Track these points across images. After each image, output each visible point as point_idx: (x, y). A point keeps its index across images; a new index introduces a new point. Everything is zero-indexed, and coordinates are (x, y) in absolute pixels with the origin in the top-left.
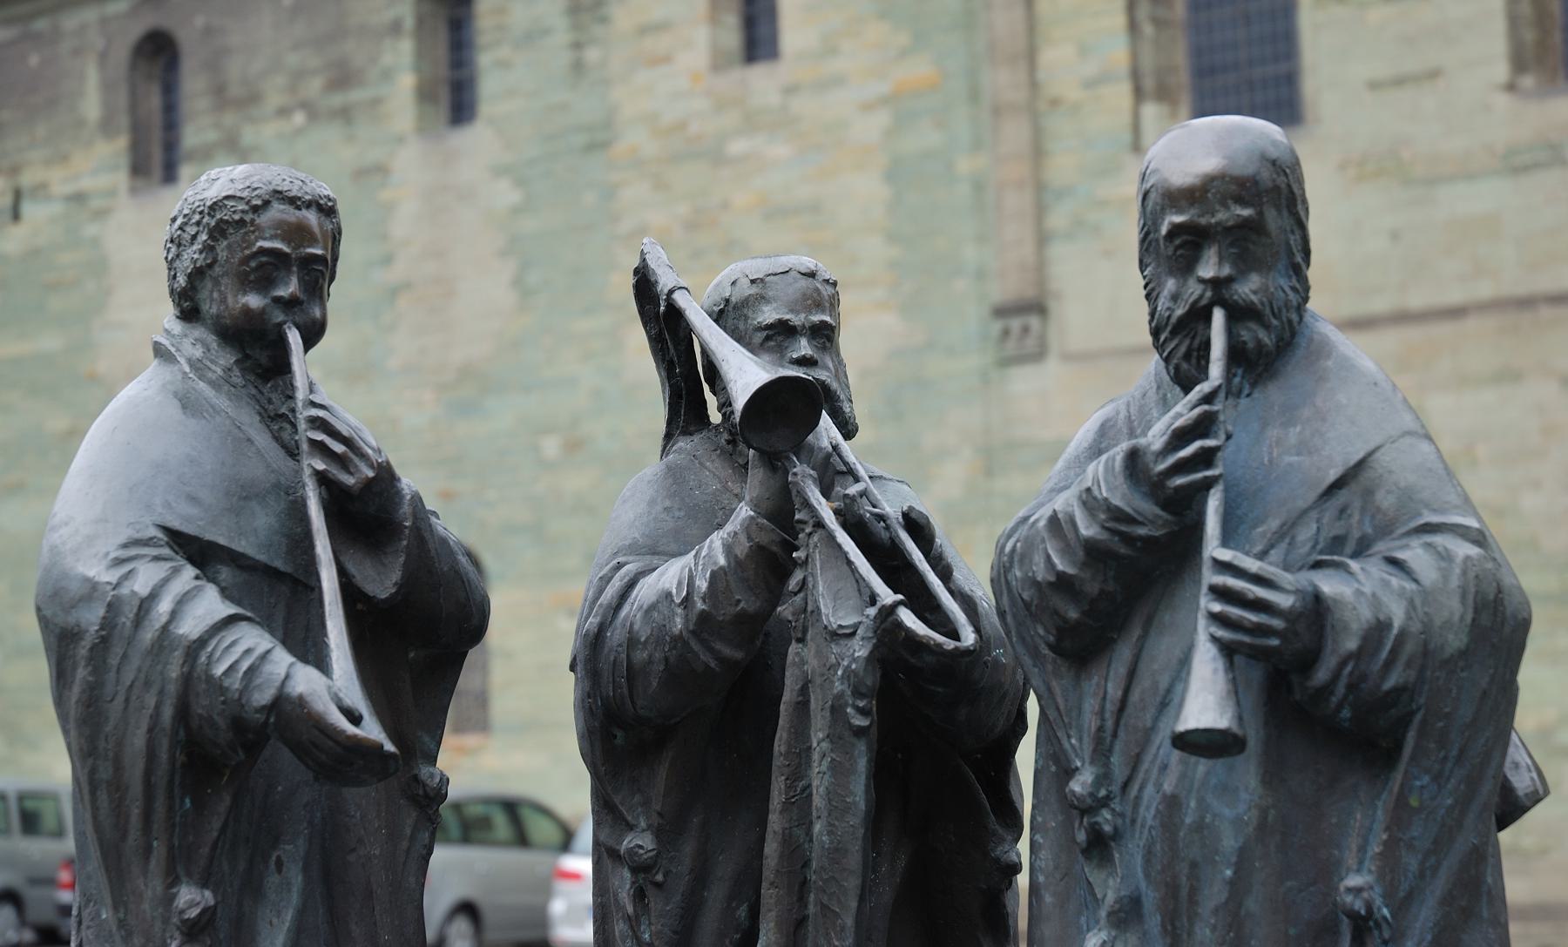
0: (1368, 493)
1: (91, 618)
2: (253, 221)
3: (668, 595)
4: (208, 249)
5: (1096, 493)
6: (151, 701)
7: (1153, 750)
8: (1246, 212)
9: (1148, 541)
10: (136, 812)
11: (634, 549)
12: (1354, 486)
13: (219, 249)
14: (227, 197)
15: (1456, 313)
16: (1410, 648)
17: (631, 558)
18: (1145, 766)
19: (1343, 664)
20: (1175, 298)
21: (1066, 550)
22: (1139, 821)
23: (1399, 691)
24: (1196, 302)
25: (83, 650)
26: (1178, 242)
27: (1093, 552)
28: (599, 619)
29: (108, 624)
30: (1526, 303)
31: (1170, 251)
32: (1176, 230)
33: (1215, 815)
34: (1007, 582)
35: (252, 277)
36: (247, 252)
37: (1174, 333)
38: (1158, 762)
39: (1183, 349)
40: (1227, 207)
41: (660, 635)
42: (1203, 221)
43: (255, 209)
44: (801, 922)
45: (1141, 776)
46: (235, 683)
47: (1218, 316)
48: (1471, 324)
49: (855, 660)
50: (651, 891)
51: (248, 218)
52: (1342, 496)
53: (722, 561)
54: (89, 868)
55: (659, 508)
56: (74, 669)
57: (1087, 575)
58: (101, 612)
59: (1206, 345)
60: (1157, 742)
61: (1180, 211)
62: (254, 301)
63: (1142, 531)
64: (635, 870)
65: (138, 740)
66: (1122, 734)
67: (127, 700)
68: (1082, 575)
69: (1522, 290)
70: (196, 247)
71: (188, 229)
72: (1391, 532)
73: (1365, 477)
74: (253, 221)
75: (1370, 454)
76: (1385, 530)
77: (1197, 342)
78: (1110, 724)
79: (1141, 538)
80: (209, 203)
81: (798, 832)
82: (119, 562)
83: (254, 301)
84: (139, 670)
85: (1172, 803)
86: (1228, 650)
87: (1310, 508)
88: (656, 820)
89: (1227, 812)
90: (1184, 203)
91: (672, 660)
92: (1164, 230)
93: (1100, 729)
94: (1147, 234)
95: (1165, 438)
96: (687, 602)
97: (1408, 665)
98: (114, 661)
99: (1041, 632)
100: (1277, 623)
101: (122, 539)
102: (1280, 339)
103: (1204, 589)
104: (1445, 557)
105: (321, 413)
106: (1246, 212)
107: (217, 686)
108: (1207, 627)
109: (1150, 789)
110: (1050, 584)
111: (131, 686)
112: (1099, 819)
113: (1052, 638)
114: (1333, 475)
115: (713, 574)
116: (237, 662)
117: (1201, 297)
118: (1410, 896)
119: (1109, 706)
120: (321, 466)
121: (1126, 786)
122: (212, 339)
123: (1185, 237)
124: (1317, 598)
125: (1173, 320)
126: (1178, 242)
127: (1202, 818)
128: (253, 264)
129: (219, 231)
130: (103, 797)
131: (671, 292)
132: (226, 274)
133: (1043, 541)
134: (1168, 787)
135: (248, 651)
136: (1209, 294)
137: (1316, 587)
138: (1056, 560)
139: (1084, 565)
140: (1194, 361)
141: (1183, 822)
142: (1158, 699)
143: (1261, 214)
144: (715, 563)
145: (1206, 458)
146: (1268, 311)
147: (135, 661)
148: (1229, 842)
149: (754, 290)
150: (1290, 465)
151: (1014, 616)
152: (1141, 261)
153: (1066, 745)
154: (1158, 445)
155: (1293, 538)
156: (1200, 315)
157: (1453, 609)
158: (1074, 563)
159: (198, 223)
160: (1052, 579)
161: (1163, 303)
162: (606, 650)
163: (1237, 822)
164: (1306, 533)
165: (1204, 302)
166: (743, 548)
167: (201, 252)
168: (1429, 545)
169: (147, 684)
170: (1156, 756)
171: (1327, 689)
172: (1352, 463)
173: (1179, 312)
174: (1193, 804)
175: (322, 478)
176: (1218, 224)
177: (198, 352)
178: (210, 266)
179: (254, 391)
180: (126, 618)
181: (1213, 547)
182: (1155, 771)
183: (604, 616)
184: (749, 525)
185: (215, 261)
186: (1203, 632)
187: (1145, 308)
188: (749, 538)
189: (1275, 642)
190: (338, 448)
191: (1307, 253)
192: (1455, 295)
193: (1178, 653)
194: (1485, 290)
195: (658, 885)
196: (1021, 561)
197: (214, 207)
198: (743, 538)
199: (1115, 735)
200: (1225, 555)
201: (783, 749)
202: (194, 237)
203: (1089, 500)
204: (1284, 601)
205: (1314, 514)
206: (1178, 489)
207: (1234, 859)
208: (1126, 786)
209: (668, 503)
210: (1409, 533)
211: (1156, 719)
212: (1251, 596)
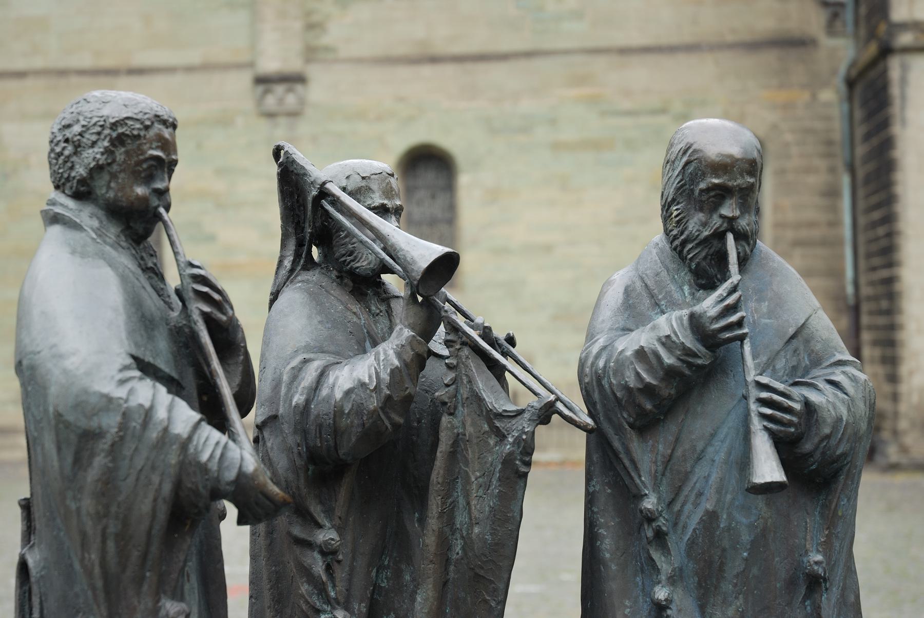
0: (807, 341)
1: (111, 422)
2: (145, 136)
3: (363, 385)
4: (107, 151)
5: (674, 338)
6: (156, 479)
7: (691, 484)
8: (752, 180)
9: (701, 367)
10: (135, 554)
11: (307, 348)
12: (800, 338)
13: (117, 154)
14: (128, 118)
15: (20, 75)
16: (849, 431)
17: (312, 356)
18: (685, 492)
19: (822, 441)
20: (704, 224)
21: (650, 370)
22: (681, 525)
23: (844, 455)
24: (717, 228)
25: (104, 445)
26: (712, 194)
27: (670, 373)
28: (303, 398)
29: (123, 426)
30: (63, 73)
33: (737, 523)
35: (143, 175)
36: (141, 157)
38: (695, 492)
39: (703, 254)
40: (743, 177)
41: (358, 410)
42: (730, 184)
43: (147, 128)
44: (445, 584)
45: (681, 499)
46: (213, 466)
47: (730, 237)
48: (29, 82)
49: (526, 433)
50: (336, 567)
51: (142, 133)
52: (795, 342)
53: (396, 362)
54: (77, 589)
55: (315, 322)
56: (92, 455)
57: (663, 385)
58: (118, 419)
60: (695, 479)
61: (717, 177)
62: (140, 190)
63: (700, 362)
64: (323, 553)
65: (145, 507)
66: (668, 474)
67: (137, 479)
68: (661, 385)
69: (62, 64)
70: (98, 149)
71: (87, 136)
72: (821, 364)
73: (806, 331)
74: (145, 136)
75: (807, 320)
76: (816, 362)
78: (660, 468)
80: (113, 121)
81: (447, 529)
82: (122, 382)
83: (140, 190)
84: (148, 459)
85: (712, 517)
86: (772, 434)
87: (781, 350)
88: (337, 522)
89: (744, 520)
91: (367, 426)
93: (656, 472)
94: (682, 186)
96: (377, 389)
97: (848, 441)
98: (127, 452)
99: (625, 416)
100: (795, 419)
101: (118, 366)
104: (853, 379)
105: (196, 271)
107: (203, 468)
108: (760, 422)
109: (689, 507)
110: (639, 389)
111: (141, 470)
112: (659, 523)
114: (791, 331)
115: (392, 371)
116: (213, 451)
117: (721, 226)
118: (834, 564)
119: (659, 458)
120: (207, 309)
121: (670, 504)
122: (101, 213)
124: (807, 404)
126: (712, 194)
127: (730, 524)
128: (145, 166)
129: (119, 141)
130: (111, 545)
131: (324, 183)
132: (123, 171)
133: (632, 363)
134: (709, 506)
135: (217, 443)
137: (806, 398)
138: (644, 375)
139: (662, 380)
140: (708, 261)
141: (719, 526)
142: (696, 456)
144: (392, 364)
145: (739, 324)
147: (144, 453)
148: (746, 537)
149: (364, 184)
150: (766, 324)
151: (604, 406)
153: (638, 481)
155: (774, 366)
156: (720, 236)
157: (861, 408)
158: (655, 378)
159: (99, 133)
160: (640, 386)
161: (693, 225)
162: (312, 417)
163: (751, 526)
164: (780, 364)
165: (722, 229)
166: (409, 355)
167: (102, 154)
168: (844, 373)
169: (153, 468)
170: (693, 488)
171: (810, 454)
174: (725, 516)
175: (207, 318)
176: (737, 186)
177: (96, 223)
178: (109, 164)
179: (134, 252)
180: (136, 424)
181: (752, 375)
182: (692, 498)
183: (308, 394)
184: (411, 341)
185: (114, 161)
186: (757, 424)
187: (661, 225)
188: (413, 349)
189: (793, 430)
190: (217, 297)
192: (20, 64)
193: (709, 430)
194: (38, 63)
195: (339, 562)
197: (114, 126)
198: (408, 348)
199: (663, 474)
200: (764, 380)
201: (440, 480)
202: (94, 144)
203: (667, 342)
204: (797, 406)
205: (782, 353)
207: (748, 547)
208: (670, 504)
209: (319, 318)
210: (831, 365)
211: (693, 467)
212: (786, 405)
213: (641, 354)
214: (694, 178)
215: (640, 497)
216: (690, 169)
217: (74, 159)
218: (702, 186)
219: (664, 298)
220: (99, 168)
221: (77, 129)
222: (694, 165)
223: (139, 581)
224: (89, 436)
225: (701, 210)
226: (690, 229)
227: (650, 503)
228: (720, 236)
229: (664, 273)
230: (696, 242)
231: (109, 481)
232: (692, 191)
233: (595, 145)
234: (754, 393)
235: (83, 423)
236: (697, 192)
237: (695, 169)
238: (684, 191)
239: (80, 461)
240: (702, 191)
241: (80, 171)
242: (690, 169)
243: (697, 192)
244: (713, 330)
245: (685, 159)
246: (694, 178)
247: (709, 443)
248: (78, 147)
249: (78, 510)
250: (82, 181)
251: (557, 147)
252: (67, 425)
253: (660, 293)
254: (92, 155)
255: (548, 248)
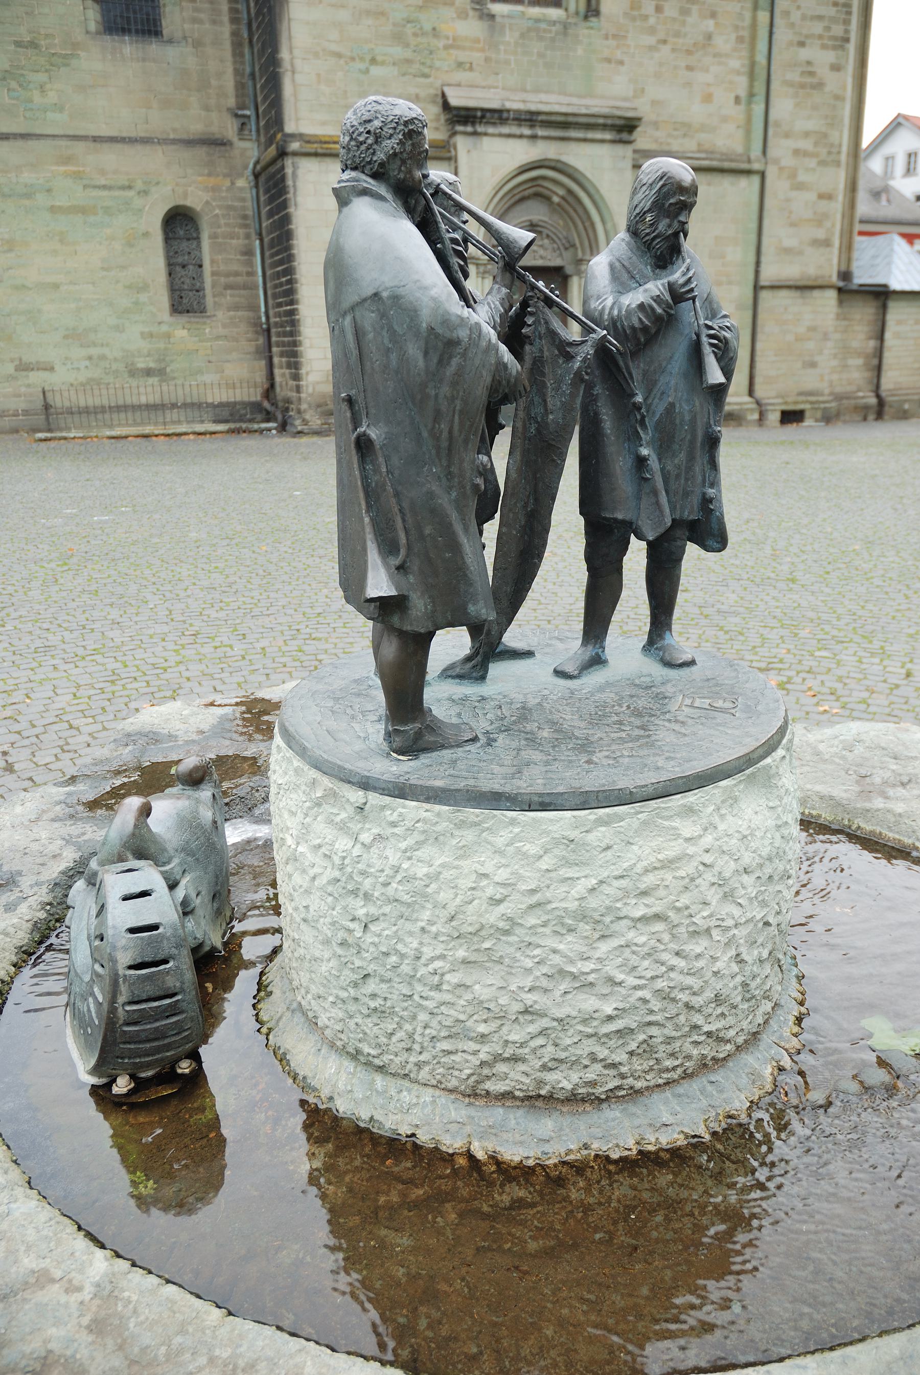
4: (401, 143)
20: (669, 226)
21: (647, 317)
25: (460, 350)
45: (652, 396)
54: (424, 449)
56: (451, 357)
70: (394, 141)
85: (672, 405)
132: (410, 158)
159: (395, 128)
197: (406, 123)
203: (657, 299)
213: (641, 306)
214: (667, 196)
215: (634, 395)
216: (665, 189)
217: (375, 147)
218: (672, 201)
220: (395, 154)
221: (377, 123)
223: (466, 441)
224: (452, 343)
225: (668, 217)
227: (639, 399)
229: (634, 258)
231: (459, 373)
232: (663, 204)
233: (83, 210)
234: (705, 332)
235: (448, 335)
239: (442, 362)
241: (381, 156)
242: (665, 189)
245: (661, 183)
246: (667, 196)
247: (669, 363)
248: (378, 139)
249: (437, 395)
250: (382, 165)
251: (53, 209)
252: (437, 336)
254: (390, 144)
255: (56, 286)
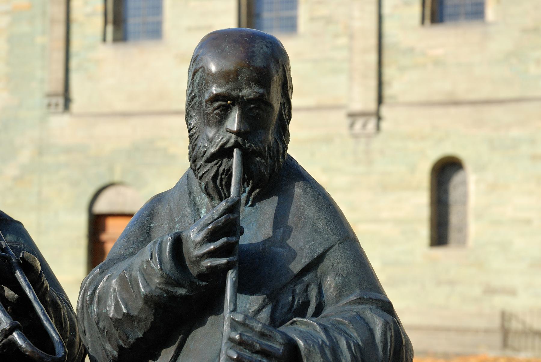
8: (261, 91)
26: (216, 105)
31: (210, 110)
32: (216, 98)
34: (88, 312)
37: (209, 161)
39: (212, 173)
40: (250, 87)
42: (234, 94)
59: (229, 172)
61: (220, 86)
63: (182, 291)
77: (221, 169)
79: (182, 297)
87: (289, 283)
90: (222, 81)
92: (207, 97)
95: (203, 234)
102: (272, 172)
103: (225, 340)
106: (261, 91)
113: (116, 353)
117: (227, 142)
123: (221, 103)
125: (208, 154)
126: (216, 105)
136: (232, 141)
140: (218, 182)
143: (269, 92)
146: (267, 154)
151: (91, 336)
152: (187, 114)
154: (199, 238)
155: (277, 302)
165: (229, 145)
172: (316, 255)
173: (213, 150)
176: (243, 97)
191: (290, 118)
196: (99, 301)
206: (208, 268)
219: (180, 221)
222: (199, 73)
226: (199, 145)
228: (224, 153)
230: (204, 159)
232: (201, 102)
236: (204, 104)
237: (202, 78)
238: (195, 103)
240: (207, 102)
243: (204, 104)
244: (197, 257)
253: (178, 216)
